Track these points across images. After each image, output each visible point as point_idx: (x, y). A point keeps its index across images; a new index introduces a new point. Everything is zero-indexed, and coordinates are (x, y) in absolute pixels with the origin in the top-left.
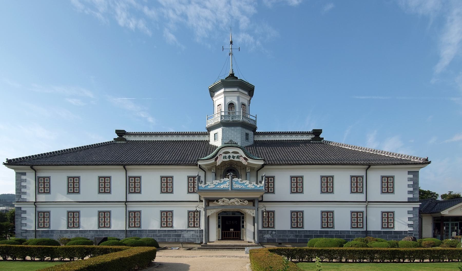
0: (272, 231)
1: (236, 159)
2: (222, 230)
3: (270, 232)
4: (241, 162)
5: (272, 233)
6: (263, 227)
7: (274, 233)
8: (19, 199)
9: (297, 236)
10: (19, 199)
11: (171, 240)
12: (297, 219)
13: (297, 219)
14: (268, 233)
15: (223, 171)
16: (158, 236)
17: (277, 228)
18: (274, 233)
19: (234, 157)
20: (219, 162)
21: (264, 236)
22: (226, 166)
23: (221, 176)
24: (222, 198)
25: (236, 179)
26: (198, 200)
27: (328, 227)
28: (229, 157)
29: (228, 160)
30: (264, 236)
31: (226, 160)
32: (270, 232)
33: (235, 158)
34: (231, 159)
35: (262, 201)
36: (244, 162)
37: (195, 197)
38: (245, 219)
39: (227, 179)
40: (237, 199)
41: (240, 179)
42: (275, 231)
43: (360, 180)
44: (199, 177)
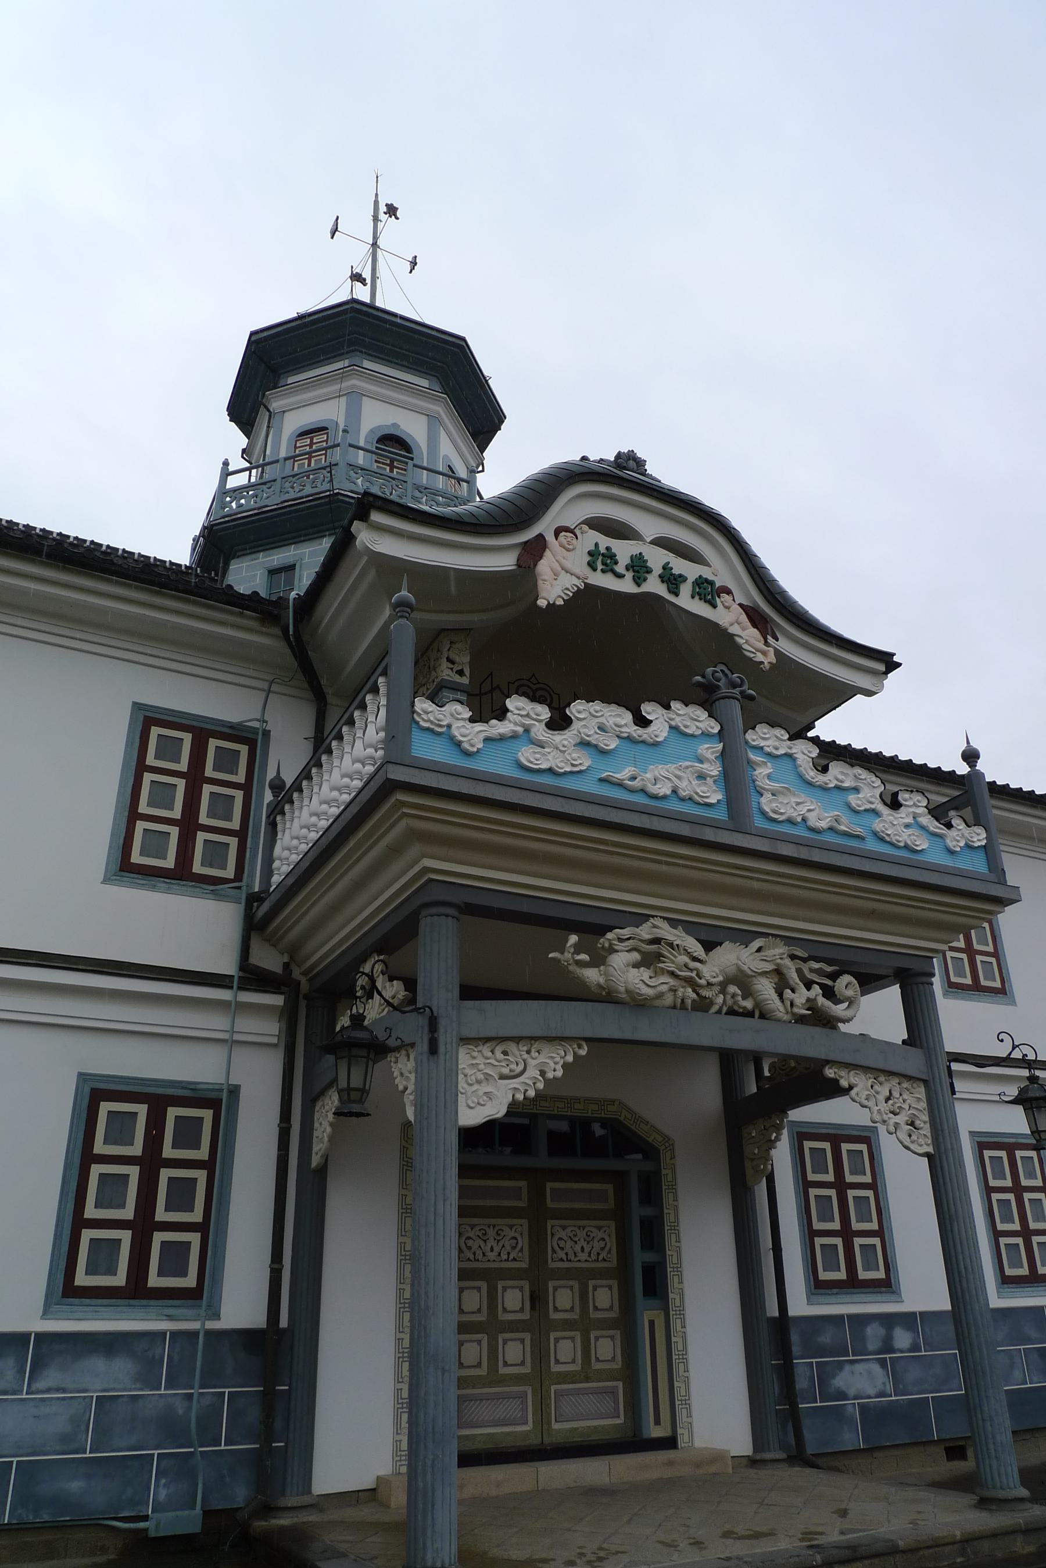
0: (889, 1321)
1: (686, 601)
5: (887, 1346)
6: (818, 1287)
7: (902, 1339)
18: (902, 1339)
19: (673, 581)
21: (840, 1381)
26: (226, 965)
29: (626, 586)
30: (840, 1381)
32: (874, 1333)
33: (686, 589)
34: (654, 586)
36: (748, 637)
37: (197, 930)
38: (668, 1198)
39: (694, 718)
42: (908, 1320)
44: (252, 739)
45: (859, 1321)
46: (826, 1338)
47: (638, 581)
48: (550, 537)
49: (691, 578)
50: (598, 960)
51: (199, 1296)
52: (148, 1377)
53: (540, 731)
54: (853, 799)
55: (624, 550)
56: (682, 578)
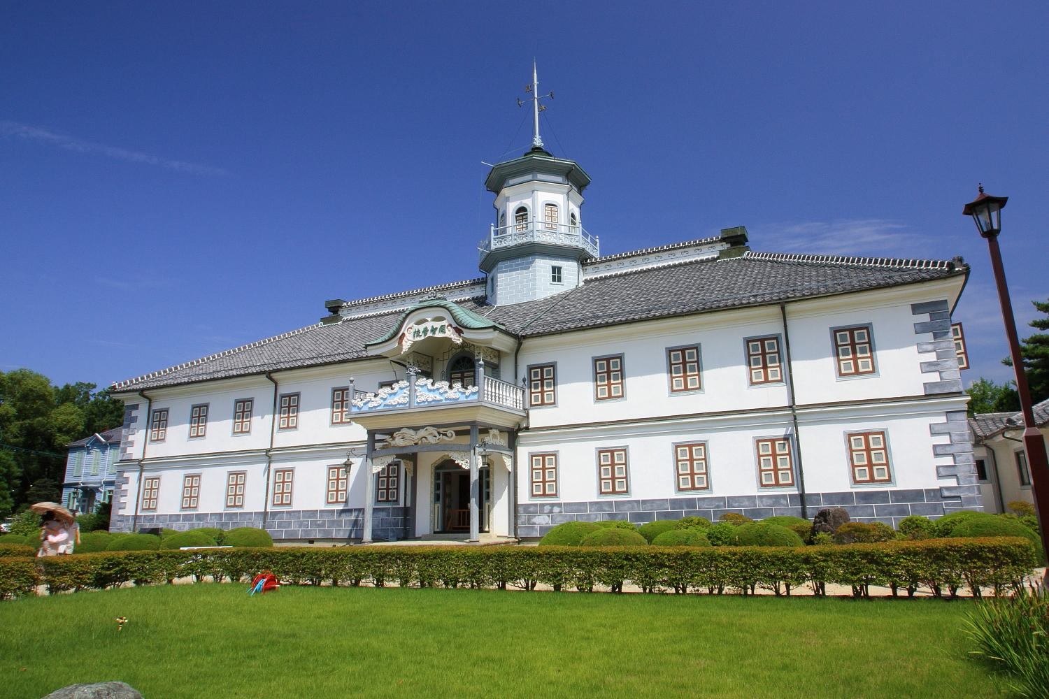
0: (553, 505)
1: (438, 335)
2: (444, 507)
3: (547, 509)
4: (450, 339)
5: (551, 512)
7: (556, 510)
8: (123, 455)
9: (612, 516)
10: (123, 455)
11: (341, 533)
12: (544, 473)
13: (544, 473)
14: (542, 512)
15: (446, 363)
16: (319, 526)
17: (564, 498)
18: (556, 510)
19: (434, 330)
20: (406, 345)
21: (534, 520)
22: (454, 350)
23: (442, 375)
24: (399, 429)
25: (423, 381)
27: (693, 488)
28: (426, 331)
29: (423, 338)
30: (534, 520)
31: (418, 339)
32: (547, 509)
33: (437, 332)
34: (430, 334)
35: (527, 429)
40: (431, 430)
41: (430, 381)
42: (559, 505)
43: (771, 346)
45: (542, 505)
46: (531, 509)
47: (425, 335)
48: (406, 333)
49: (439, 327)
50: (393, 438)
51: (397, 501)
52: (388, 515)
53: (373, 399)
54: (441, 391)
55: (421, 327)
56: (436, 328)
